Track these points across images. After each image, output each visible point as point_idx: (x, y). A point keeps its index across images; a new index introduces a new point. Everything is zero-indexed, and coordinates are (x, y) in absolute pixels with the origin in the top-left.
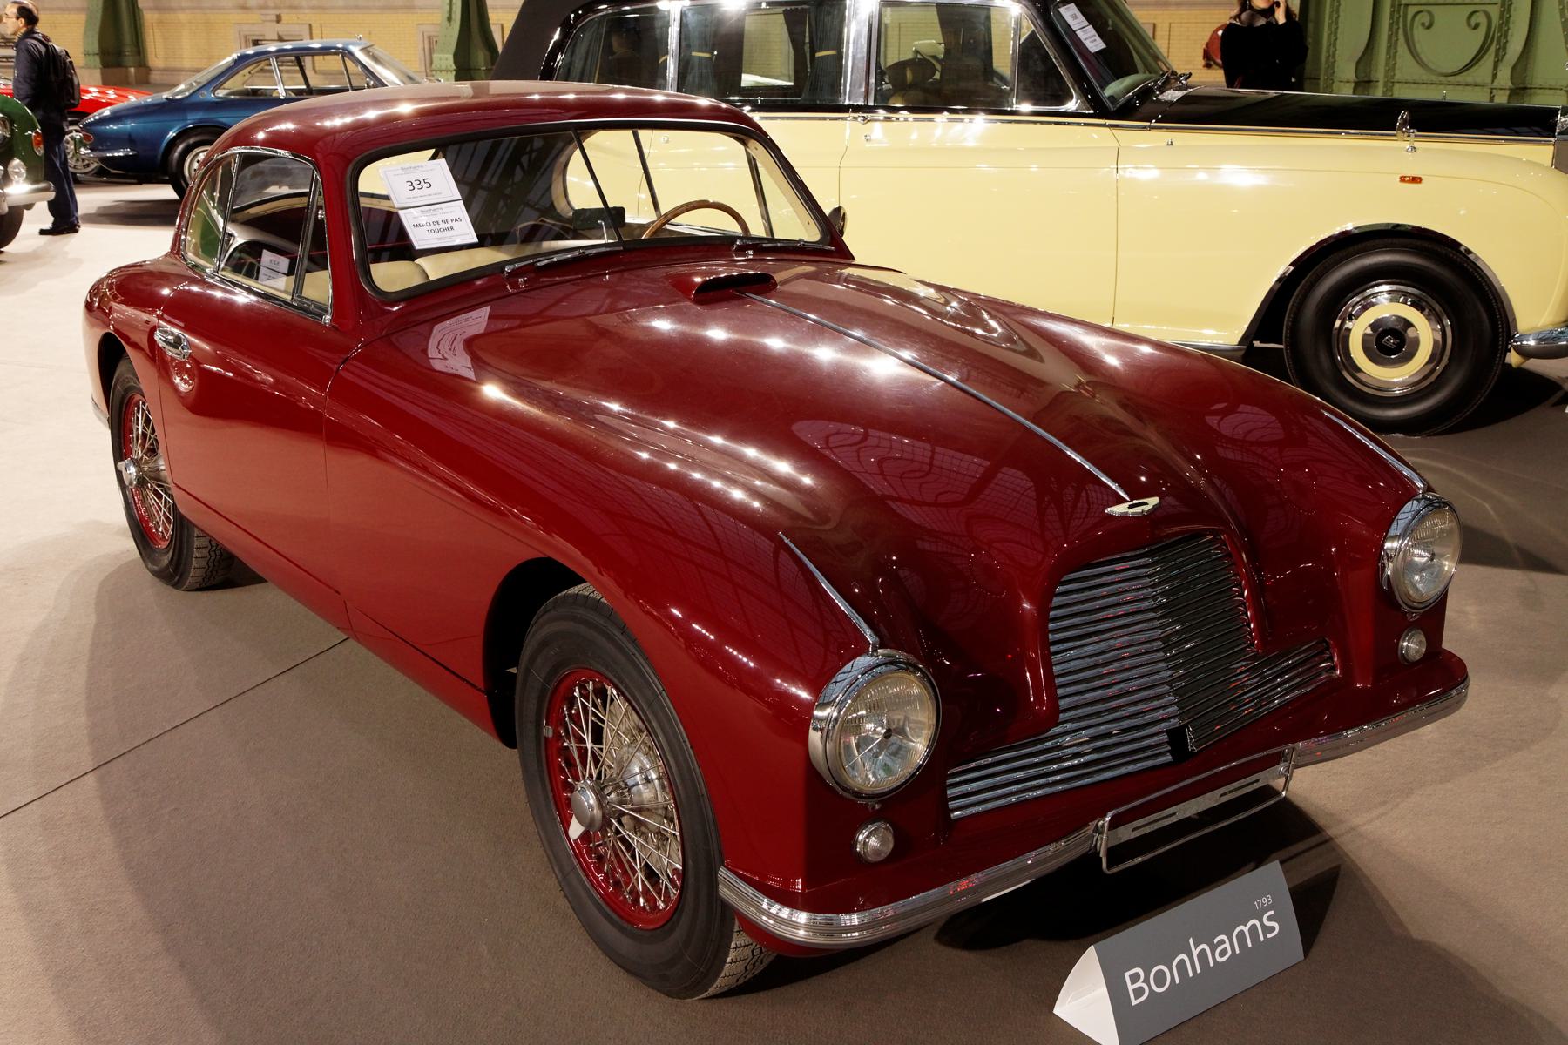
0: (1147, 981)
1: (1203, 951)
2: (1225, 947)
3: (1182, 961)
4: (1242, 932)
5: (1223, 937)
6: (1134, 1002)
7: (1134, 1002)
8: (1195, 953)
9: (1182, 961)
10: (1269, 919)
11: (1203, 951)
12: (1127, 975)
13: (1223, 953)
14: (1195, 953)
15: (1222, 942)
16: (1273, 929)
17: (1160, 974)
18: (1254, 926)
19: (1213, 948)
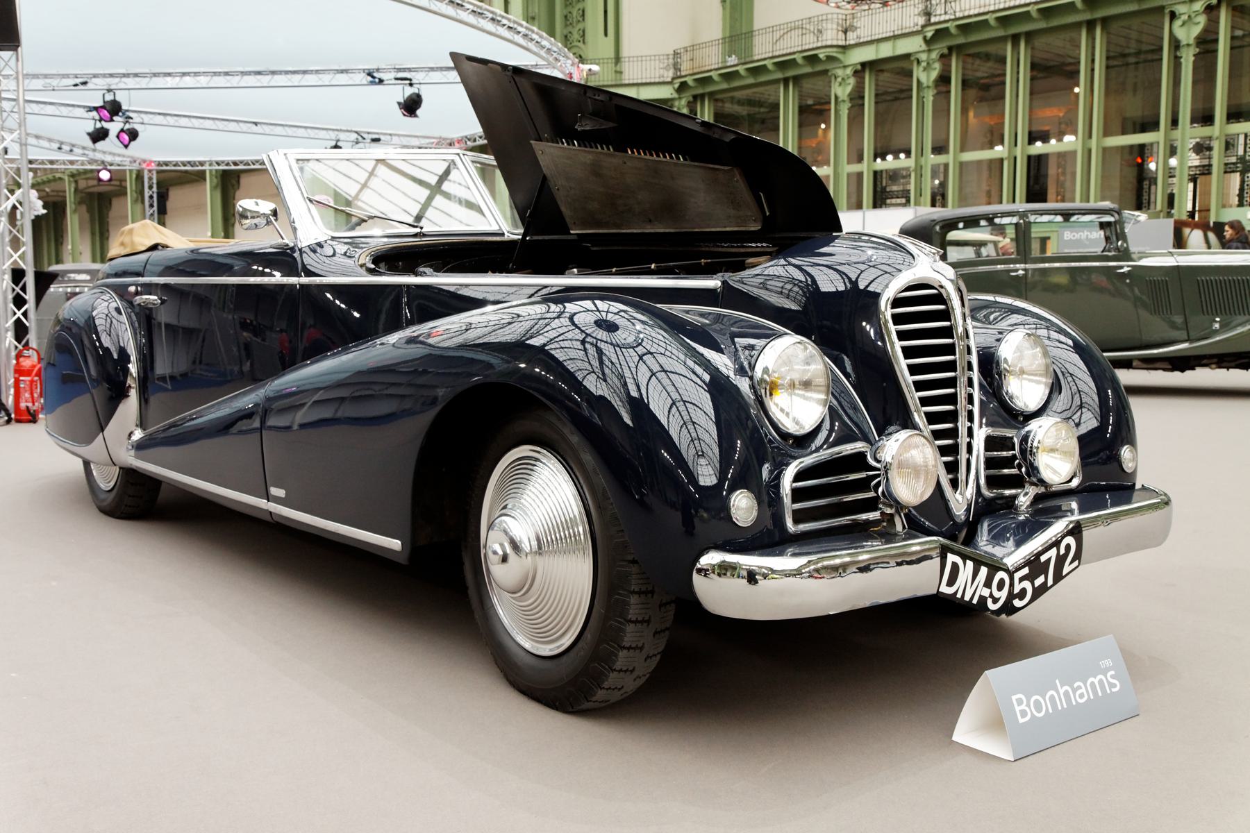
2: (1082, 693)
3: (1052, 698)
8: (1062, 691)
10: (1112, 677)
11: (1066, 693)
13: (1082, 696)
14: (1062, 691)
15: (1079, 687)
16: (1115, 686)
17: (1037, 702)
19: (1074, 691)
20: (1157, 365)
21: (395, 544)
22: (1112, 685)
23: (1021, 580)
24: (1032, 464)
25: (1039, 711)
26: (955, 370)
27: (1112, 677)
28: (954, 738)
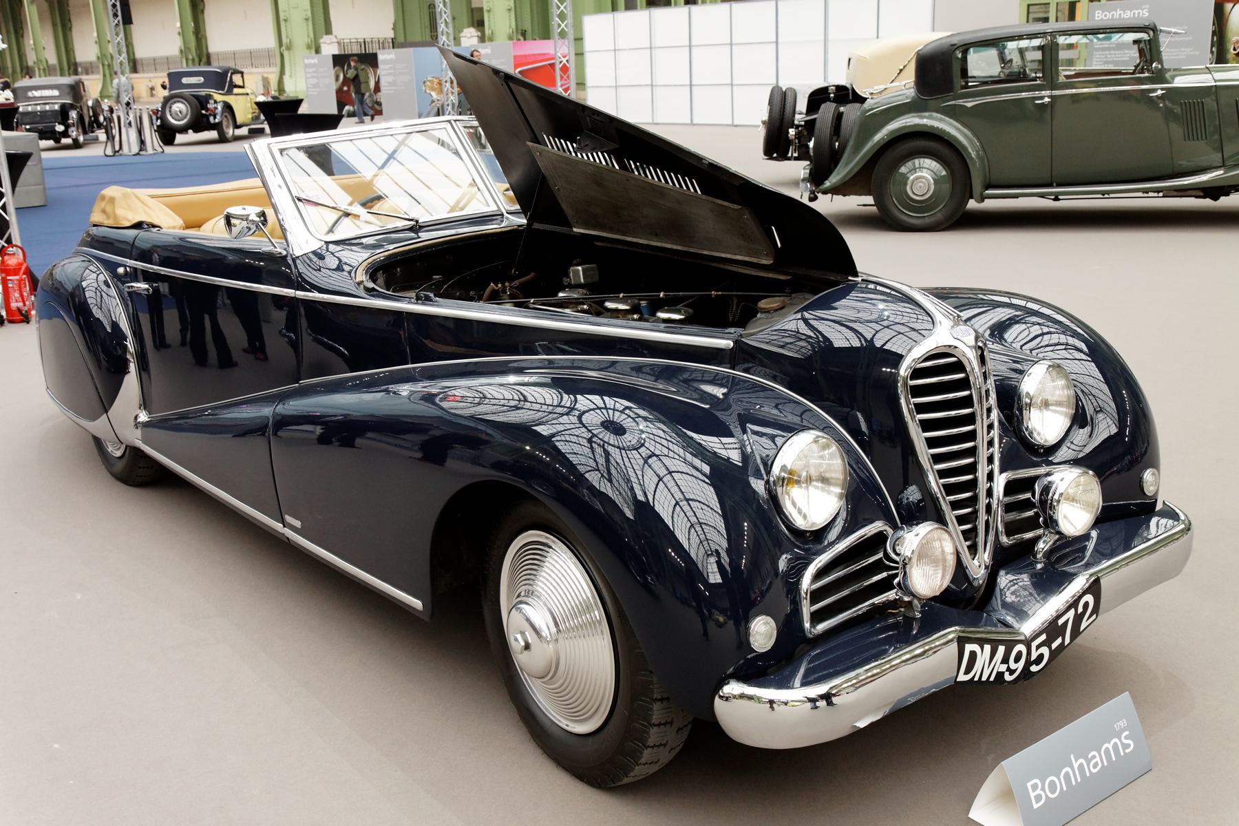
0: (1043, 789)
2: (1096, 762)
3: (1067, 773)
4: (1107, 749)
5: (1094, 753)
6: (1036, 806)
7: (1036, 806)
8: (1076, 766)
9: (1067, 773)
10: (1126, 738)
13: (1095, 765)
14: (1076, 766)
15: (1094, 757)
16: (1128, 746)
17: (1052, 784)
18: (1115, 744)
20: (1189, 193)
21: (417, 604)
22: (1126, 746)
23: (1038, 647)
24: (1051, 517)
25: (1053, 790)
26: (972, 406)
27: (1126, 738)
28: (971, 815)
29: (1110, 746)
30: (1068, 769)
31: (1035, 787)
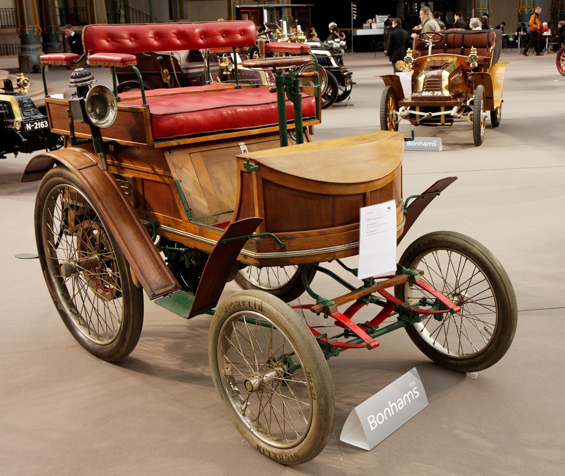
0: (376, 420)
1: (394, 406)
3: (387, 411)
6: (372, 429)
7: (372, 429)
8: (391, 407)
9: (387, 411)
10: (415, 390)
11: (394, 406)
12: (368, 418)
13: (401, 406)
14: (391, 407)
15: (400, 401)
16: (416, 394)
17: (380, 416)
18: (410, 394)
29: (407, 395)
30: (387, 409)
31: (371, 419)
